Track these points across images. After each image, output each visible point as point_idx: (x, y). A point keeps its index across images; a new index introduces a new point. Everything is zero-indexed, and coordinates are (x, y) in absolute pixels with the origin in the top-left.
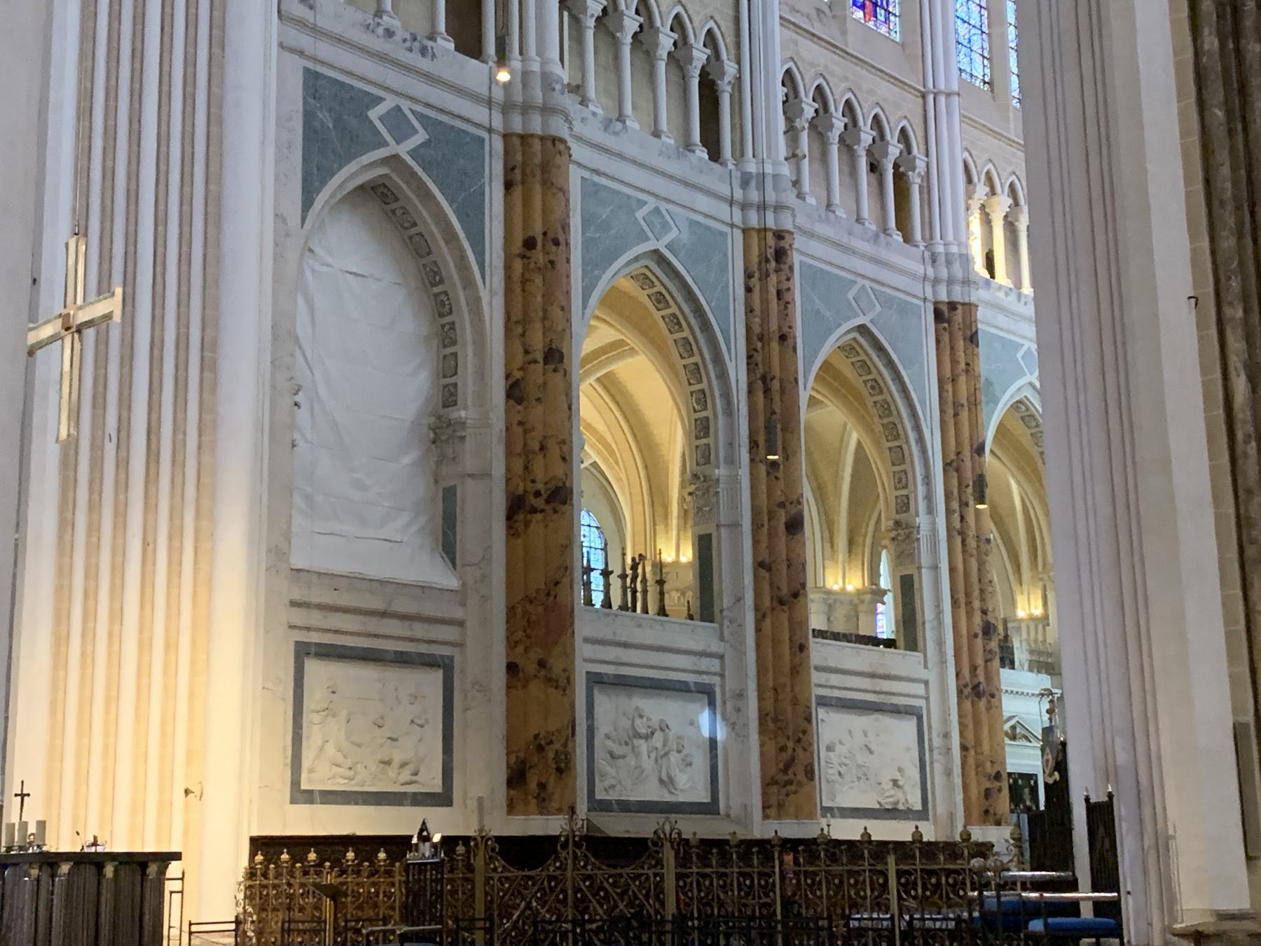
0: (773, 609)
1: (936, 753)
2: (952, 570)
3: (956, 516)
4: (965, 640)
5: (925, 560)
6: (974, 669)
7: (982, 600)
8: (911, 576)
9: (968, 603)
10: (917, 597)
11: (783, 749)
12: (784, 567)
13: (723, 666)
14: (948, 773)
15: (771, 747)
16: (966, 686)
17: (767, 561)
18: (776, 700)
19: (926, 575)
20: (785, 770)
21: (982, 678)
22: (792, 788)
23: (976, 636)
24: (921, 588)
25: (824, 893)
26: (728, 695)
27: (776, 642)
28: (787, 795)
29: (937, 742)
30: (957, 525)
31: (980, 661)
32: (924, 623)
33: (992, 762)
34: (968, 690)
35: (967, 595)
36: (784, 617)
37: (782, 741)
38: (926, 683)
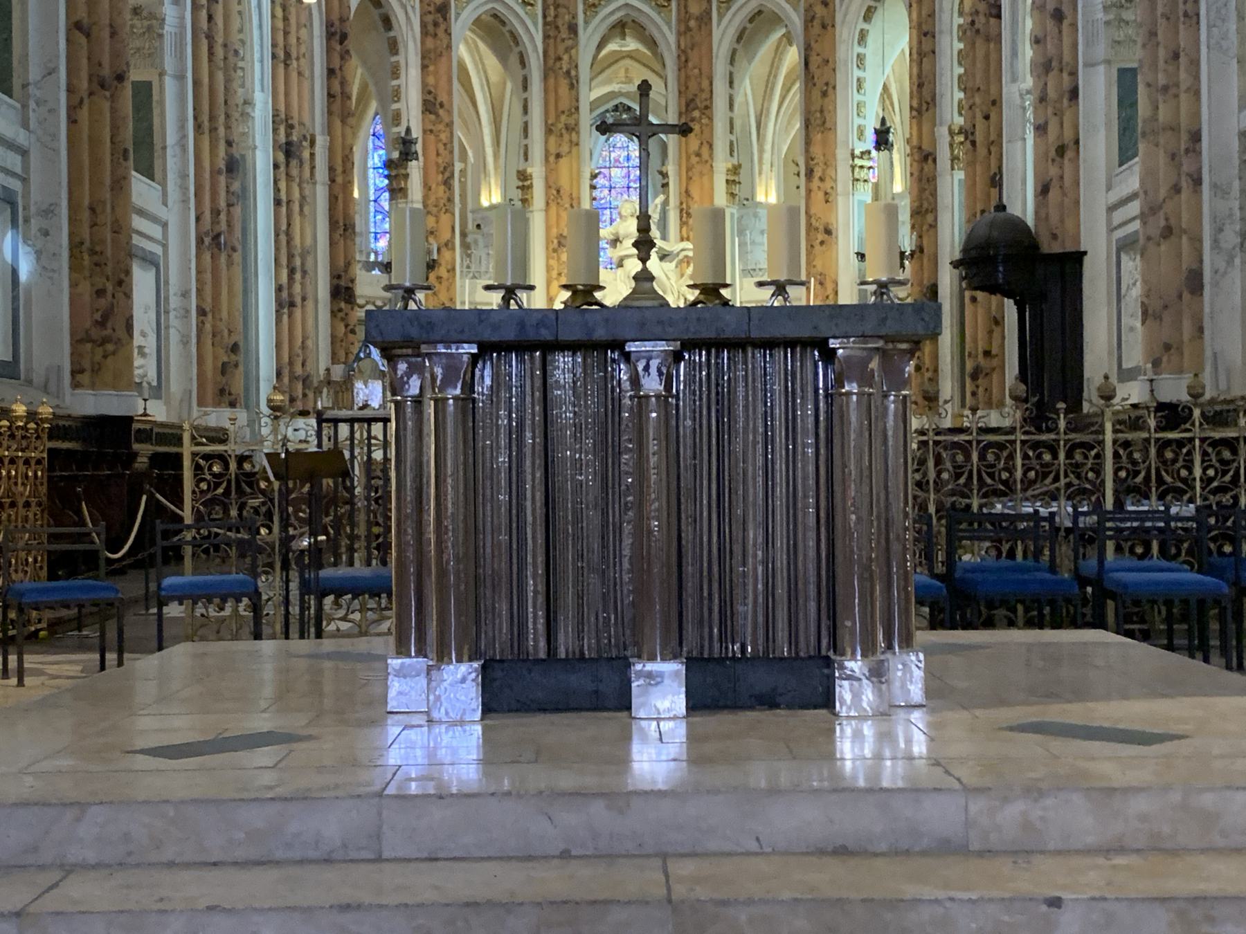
0: (91, 94)
1: (172, 315)
2: (197, 83)
3: (204, 13)
4: (207, 175)
5: (169, 64)
6: (216, 212)
7: (228, 127)
8: (149, 84)
9: (213, 130)
10: (156, 112)
11: (100, 293)
12: (106, 33)
13: (26, 167)
14: (185, 342)
15: (85, 288)
16: (207, 234)
17: (85, 21)
18: (93, 225)
19: (170, 84)
20: (102, 324)
21: (223, 226)
22: (110, 347)
23: (219, 172)
24: (162, 103)
25: (1198, 472)
26: (33, 209)
27: (94, 142)
28: (105, 357)
29: (174, 302)
30: (204, 24)
31: (222, 204)
32: (164, 148)
33: (230, 332)
34: (207, 240)
35: (212, 118)
36: (106, 105)
37: (100, 282)
38: (165, 225)
